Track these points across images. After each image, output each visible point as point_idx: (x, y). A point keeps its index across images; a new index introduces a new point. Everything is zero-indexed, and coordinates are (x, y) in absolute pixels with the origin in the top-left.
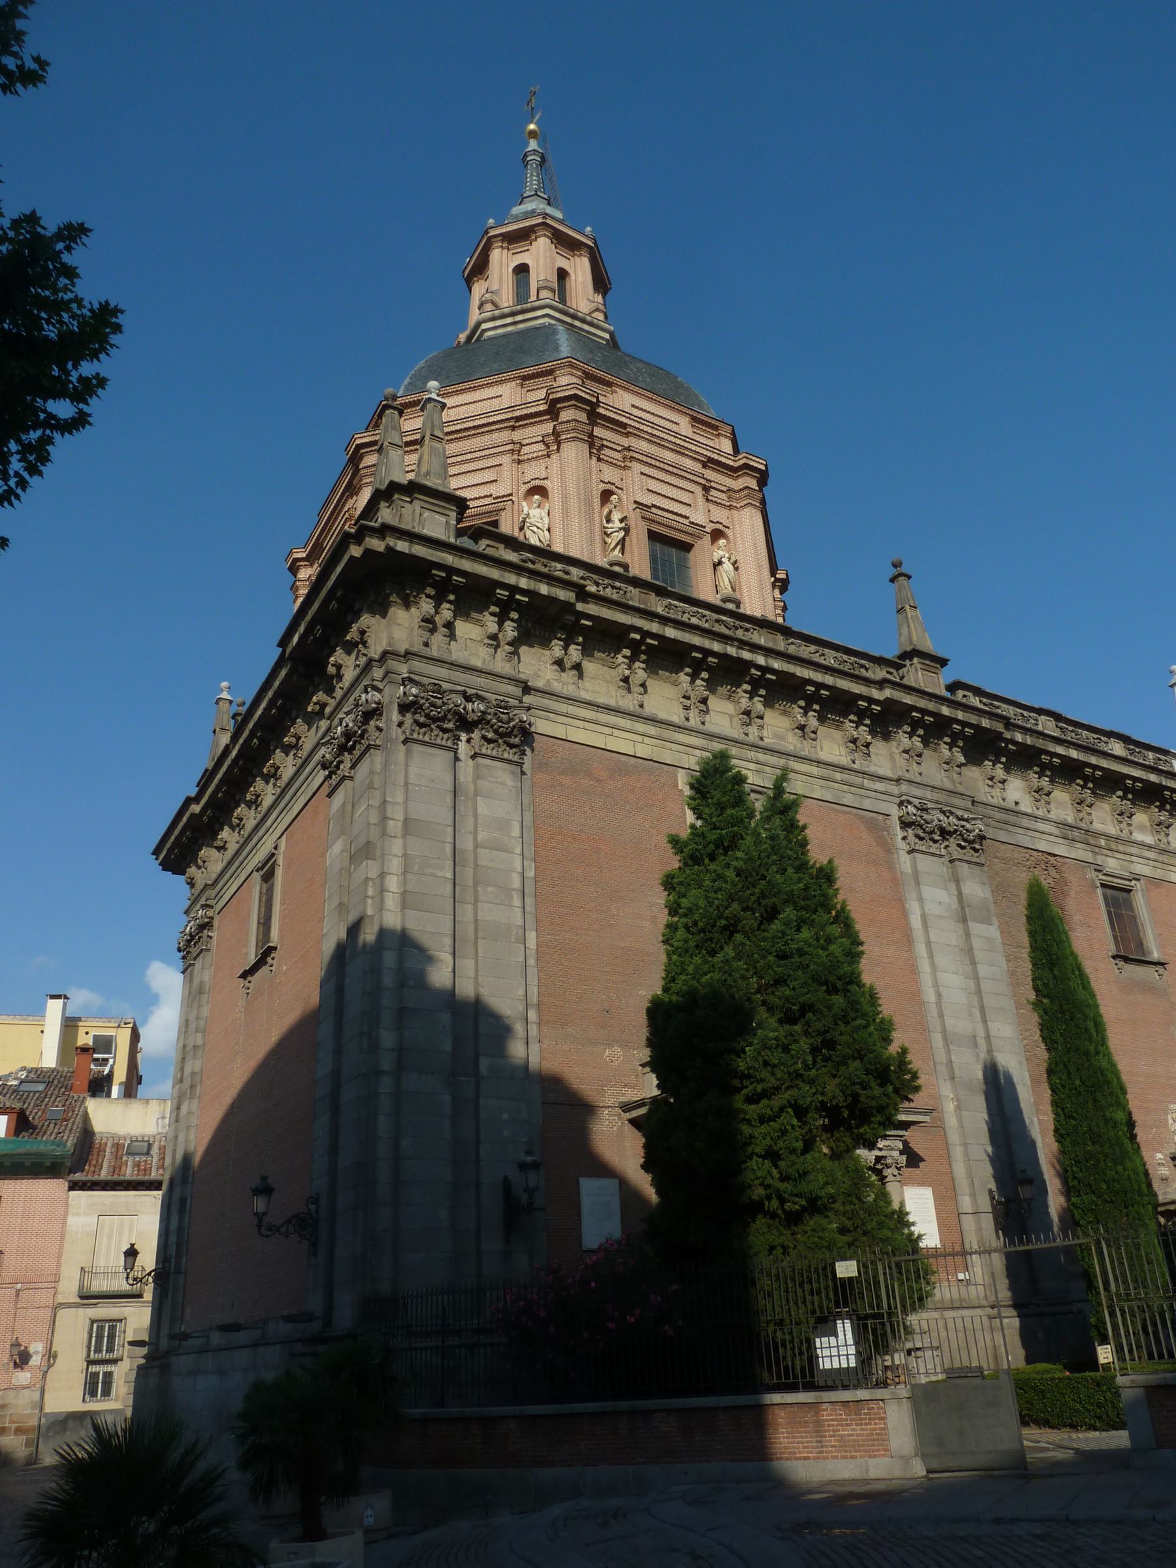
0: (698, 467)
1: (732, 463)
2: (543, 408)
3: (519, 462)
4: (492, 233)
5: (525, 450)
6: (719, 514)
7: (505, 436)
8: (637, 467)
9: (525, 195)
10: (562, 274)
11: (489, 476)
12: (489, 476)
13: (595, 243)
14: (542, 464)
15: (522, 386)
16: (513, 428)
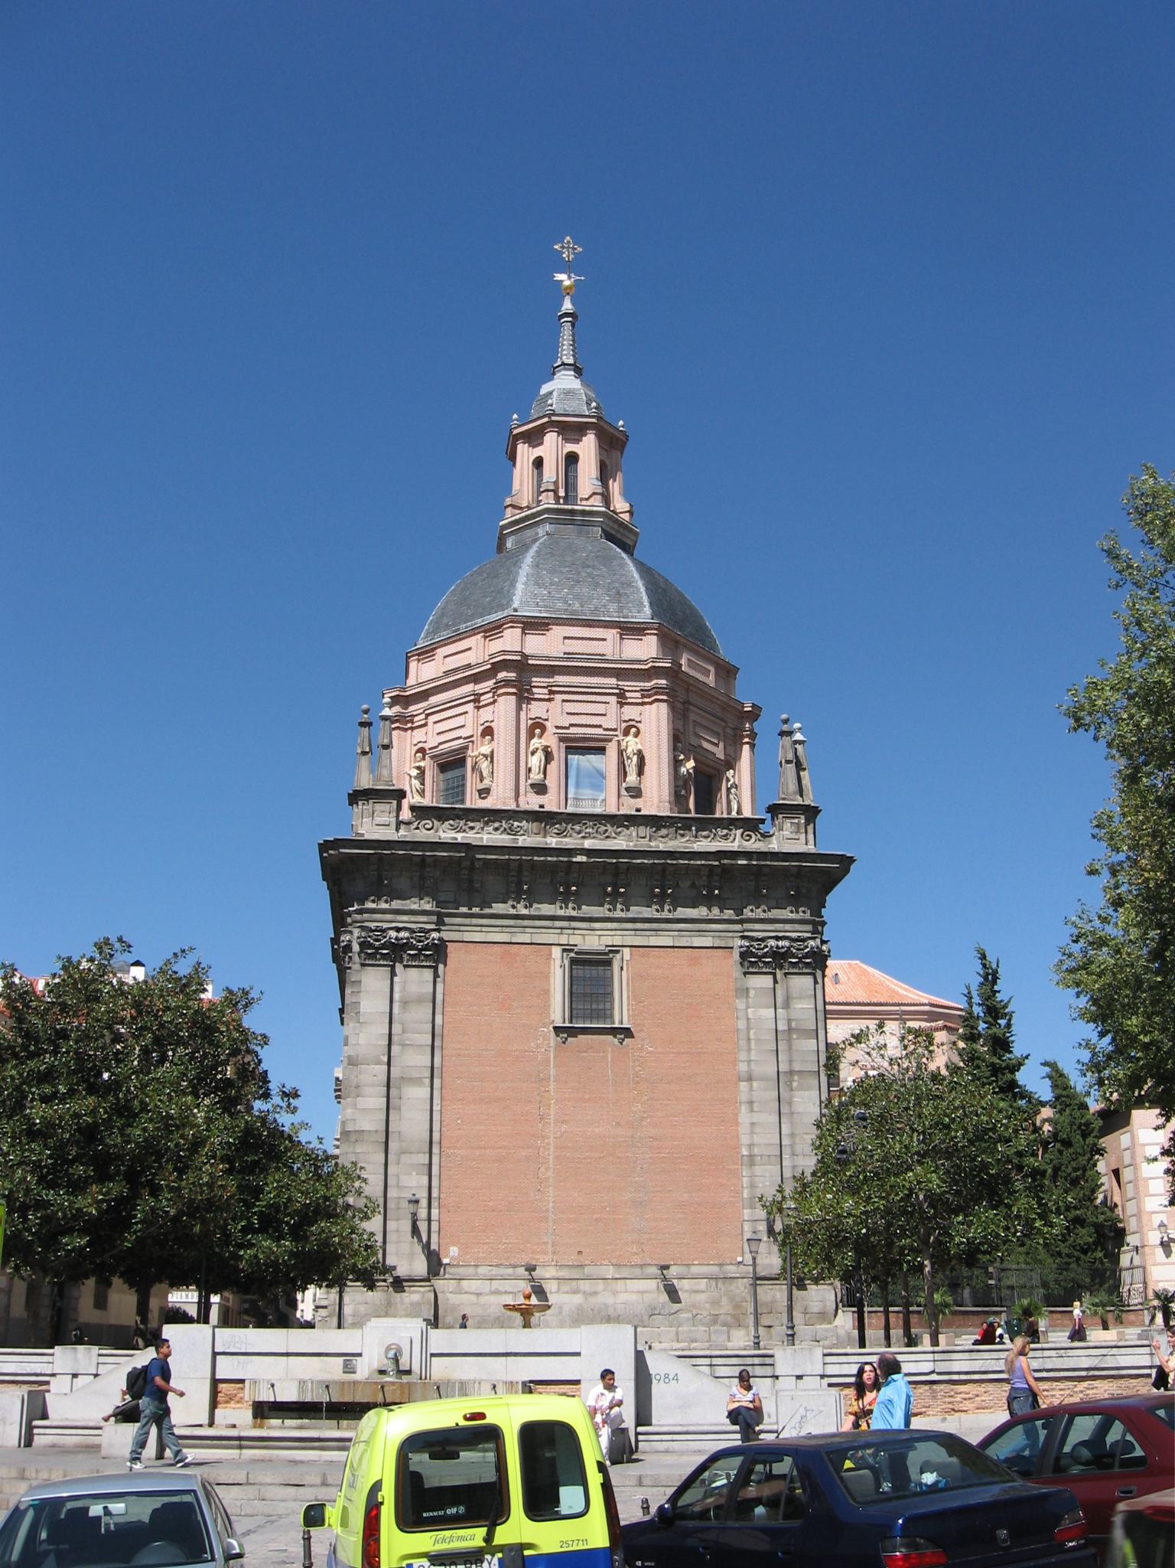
0: (613, 681)
1: (643, 667)
2: (489, 666)
3: (478, 708)
4: (515, 432)
5: (482, 698)
6: (630, 712)
7: (468, 688)
8: (559, 697)
9: (555, 365)
10: (572, 459)
11: (459, 721)
12: (459, 721)
13: (599, 418)
14: (490, 708)
15: (485, 637)
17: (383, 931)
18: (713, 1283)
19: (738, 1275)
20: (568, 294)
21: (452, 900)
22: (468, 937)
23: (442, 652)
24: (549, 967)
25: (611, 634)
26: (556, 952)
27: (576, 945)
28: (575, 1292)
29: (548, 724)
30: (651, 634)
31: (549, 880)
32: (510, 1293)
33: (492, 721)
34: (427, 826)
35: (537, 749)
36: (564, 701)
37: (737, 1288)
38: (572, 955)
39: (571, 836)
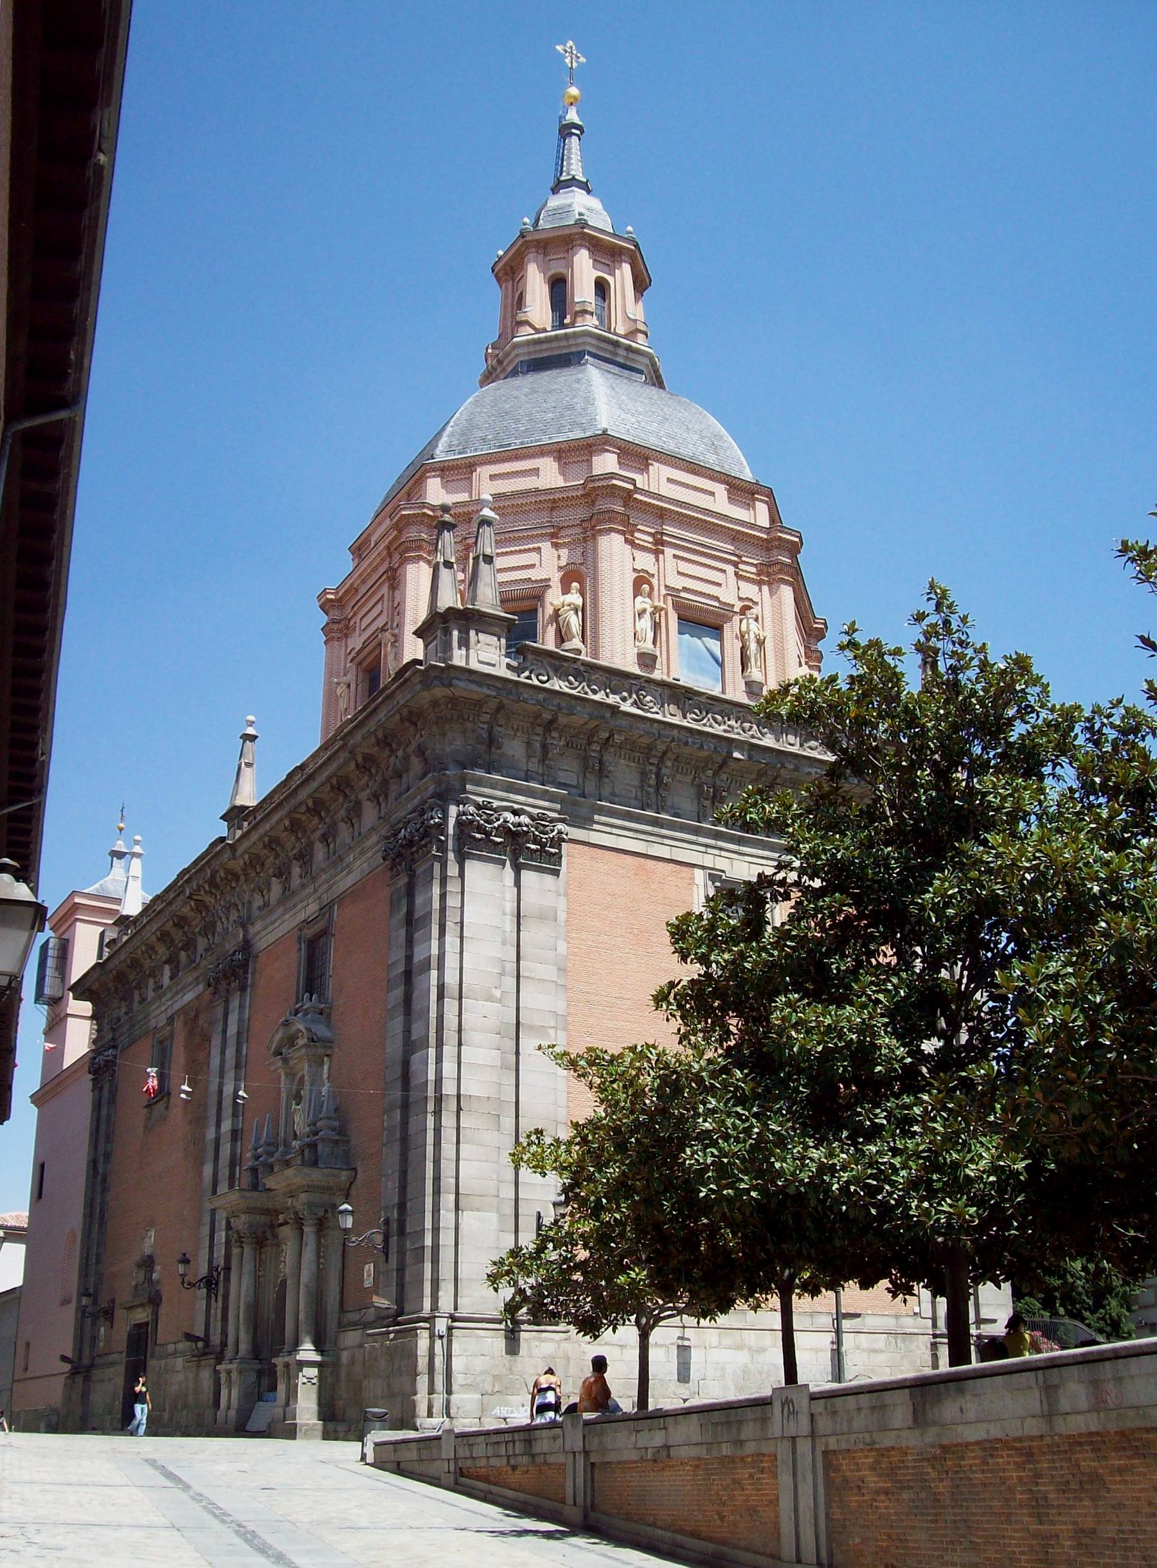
5: (562, 533)
6: (749, 590)
8: (669, 552)
16: (552, 509)
17: (495, 810)
18: (892, 1339)
19: (916, 1331)
20: (572, 104)
21: (574, 783)
22: (594, 838)
23: (484, 471)
24: (692, 895)
25: (720, 489)
26: (699, 875)
27: (723, 871)
28: (739, 1347)
29: (655, 581)
30: (761, 501)
31: (691, 777)
32: (661, 1346)
33: (581, 564)
34: (541, 678)
35: (644, 611)
36: (675, 556)
37: (917, 1347)
38: (718, 884)
39: (711, 726)
